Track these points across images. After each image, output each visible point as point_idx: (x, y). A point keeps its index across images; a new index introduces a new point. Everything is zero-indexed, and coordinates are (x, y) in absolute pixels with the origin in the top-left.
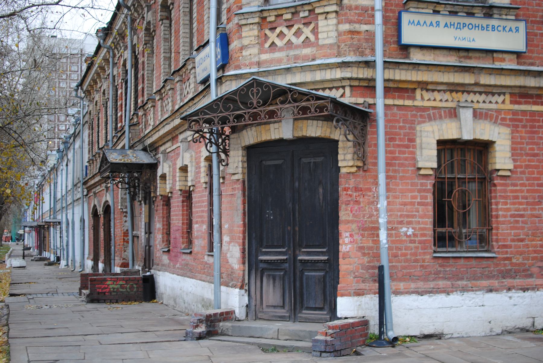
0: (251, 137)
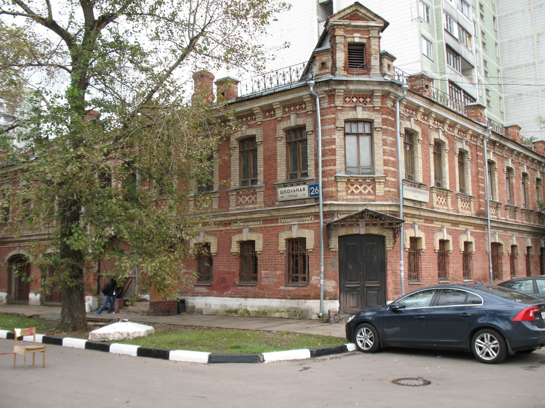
0: (343, 232)
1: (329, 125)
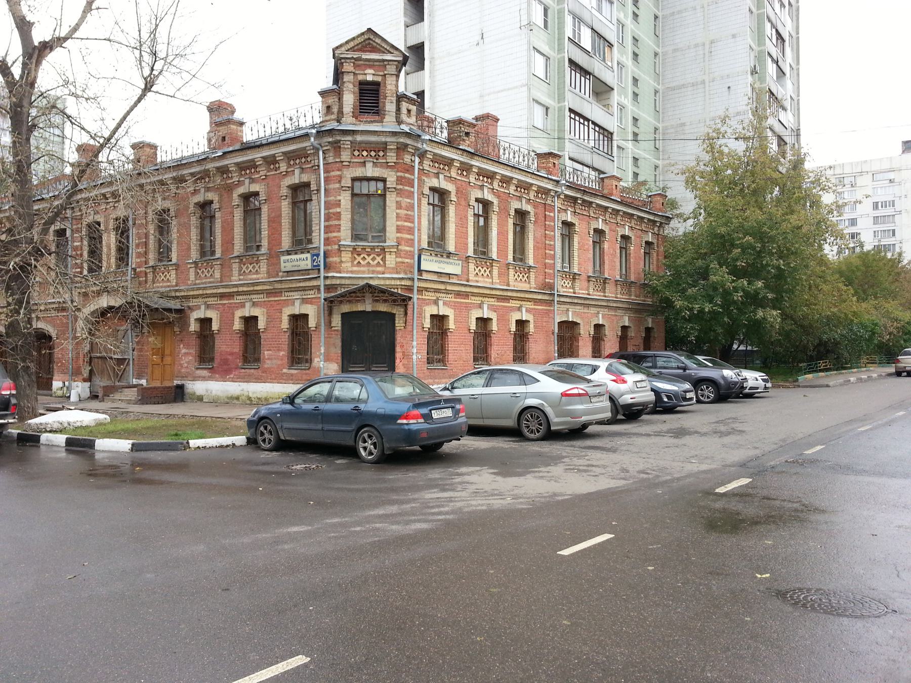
0: (346, 308)
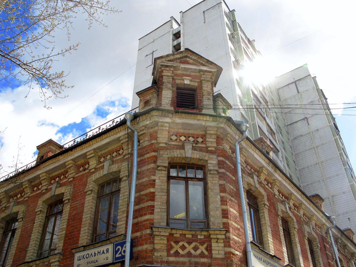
1: (148, 164)
